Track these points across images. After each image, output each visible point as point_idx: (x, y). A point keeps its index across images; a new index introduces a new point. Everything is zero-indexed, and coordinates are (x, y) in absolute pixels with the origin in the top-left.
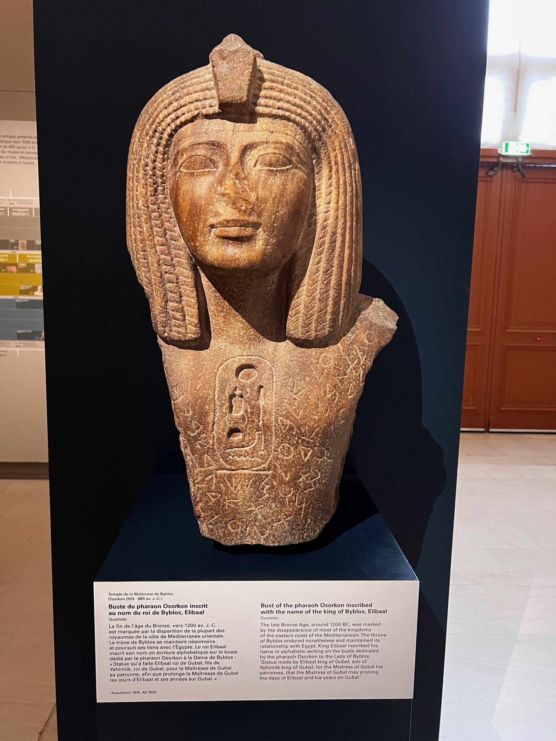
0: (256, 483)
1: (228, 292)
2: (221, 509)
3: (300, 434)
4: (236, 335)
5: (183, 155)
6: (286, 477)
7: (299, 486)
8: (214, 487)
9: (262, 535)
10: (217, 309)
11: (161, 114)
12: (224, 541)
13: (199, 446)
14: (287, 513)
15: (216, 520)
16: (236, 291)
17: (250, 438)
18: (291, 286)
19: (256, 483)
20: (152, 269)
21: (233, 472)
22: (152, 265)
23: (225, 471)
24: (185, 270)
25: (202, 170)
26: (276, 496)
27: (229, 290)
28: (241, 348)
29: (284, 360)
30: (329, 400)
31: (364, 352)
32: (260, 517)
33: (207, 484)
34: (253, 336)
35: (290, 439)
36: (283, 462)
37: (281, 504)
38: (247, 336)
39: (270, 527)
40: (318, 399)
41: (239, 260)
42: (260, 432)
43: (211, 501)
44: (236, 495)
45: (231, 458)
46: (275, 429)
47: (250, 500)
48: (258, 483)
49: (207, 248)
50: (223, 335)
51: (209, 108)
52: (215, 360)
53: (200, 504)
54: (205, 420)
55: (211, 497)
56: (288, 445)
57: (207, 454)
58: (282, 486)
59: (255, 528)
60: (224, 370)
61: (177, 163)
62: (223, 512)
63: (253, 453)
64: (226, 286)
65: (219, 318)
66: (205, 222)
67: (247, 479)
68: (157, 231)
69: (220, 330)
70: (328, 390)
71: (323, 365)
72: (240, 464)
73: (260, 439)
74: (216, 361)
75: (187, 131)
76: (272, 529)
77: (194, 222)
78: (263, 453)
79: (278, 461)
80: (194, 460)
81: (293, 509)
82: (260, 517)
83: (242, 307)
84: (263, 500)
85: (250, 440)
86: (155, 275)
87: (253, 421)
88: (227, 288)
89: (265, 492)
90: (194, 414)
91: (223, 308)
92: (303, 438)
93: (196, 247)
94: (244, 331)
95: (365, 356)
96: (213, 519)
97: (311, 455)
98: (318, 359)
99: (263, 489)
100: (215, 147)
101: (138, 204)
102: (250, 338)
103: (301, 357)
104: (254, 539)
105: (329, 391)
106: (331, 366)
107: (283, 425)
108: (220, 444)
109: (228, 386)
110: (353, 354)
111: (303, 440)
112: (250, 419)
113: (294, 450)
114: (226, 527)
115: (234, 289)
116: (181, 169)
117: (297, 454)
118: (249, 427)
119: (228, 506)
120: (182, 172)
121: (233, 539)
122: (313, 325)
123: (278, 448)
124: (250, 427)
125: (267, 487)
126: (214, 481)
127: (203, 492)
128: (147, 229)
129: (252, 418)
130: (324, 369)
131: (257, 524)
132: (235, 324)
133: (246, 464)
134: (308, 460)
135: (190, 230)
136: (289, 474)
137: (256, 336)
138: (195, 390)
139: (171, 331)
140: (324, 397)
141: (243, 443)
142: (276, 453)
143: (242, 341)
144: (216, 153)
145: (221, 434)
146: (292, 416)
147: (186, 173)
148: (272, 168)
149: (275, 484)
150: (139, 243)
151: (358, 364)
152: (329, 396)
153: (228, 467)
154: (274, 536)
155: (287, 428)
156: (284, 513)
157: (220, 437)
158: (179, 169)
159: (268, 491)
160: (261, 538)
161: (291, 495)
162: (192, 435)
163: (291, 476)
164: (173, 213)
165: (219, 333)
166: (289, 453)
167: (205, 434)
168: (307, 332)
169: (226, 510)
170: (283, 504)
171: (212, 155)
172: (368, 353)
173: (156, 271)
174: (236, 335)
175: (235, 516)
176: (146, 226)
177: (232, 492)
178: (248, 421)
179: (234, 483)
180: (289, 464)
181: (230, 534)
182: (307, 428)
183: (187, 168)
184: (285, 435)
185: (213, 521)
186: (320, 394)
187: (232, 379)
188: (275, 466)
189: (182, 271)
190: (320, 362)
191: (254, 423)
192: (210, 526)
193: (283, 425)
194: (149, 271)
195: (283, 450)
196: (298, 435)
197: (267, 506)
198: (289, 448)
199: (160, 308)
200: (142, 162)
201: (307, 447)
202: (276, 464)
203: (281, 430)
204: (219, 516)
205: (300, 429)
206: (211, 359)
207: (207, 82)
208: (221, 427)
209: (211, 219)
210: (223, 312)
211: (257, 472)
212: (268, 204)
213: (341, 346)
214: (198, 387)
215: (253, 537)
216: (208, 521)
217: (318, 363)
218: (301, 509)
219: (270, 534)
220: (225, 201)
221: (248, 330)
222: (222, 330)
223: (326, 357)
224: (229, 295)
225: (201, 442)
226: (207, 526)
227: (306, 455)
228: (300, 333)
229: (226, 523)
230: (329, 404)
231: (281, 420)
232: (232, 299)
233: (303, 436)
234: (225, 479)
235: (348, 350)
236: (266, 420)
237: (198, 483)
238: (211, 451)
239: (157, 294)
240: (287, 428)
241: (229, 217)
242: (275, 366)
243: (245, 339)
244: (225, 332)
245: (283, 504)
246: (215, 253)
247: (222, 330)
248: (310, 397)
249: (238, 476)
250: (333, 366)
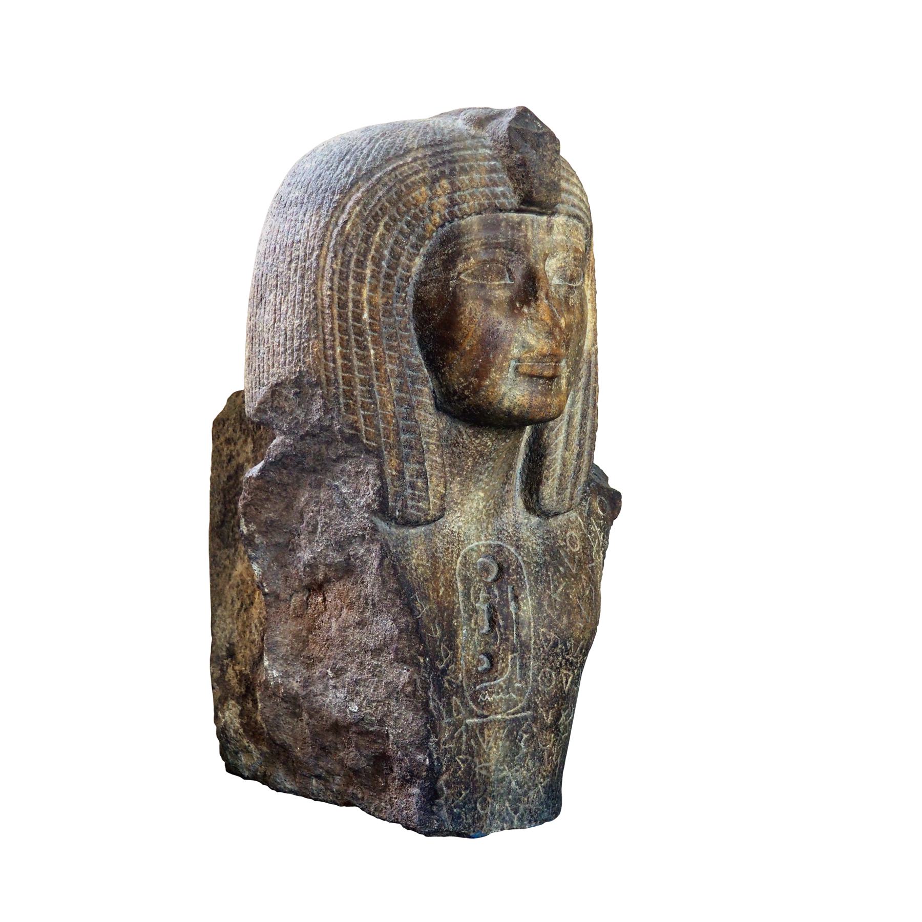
0: (512, 734)
1: (476, 447)
2: (472, 780)
3: (566, 651)
4: (473, 510)
5: (470, 259)
6: (548, 718)
7: (559, 731)
8: (463, 747)
9: (515, 813)
10: (451, 472)
11: (417, 192)
12: (474, 831)
13: (446, 685)
14: (544, 773)
15: (464, 798)
16: (489, 445)
17: (504, 665)
18: (548, 437)
19: (513, 734)
20: (382, 413)
21: (485, 720)
22: (384, 406)
23: (476, 720)
24: (428, 415)
25: (497, 283)
26: (535, 750)
27: (479, 443)
28: (478, 529)
29: (530, 544)
30: (588, 598)
31: (601, 527)
32: (513, 783)
33: (456, 744)
34: (492, 511)
35: (553, 661)
36: (545, 696)
37: (540, 761)
38: (487, 511)
39: (526, 799)
40: (579, 598)
41: (551, 406)
42: (515, 654)
43: (460, 769)
44: (489, 755)
45: (483, 699)
46: (534, 648)
47: (504, 761)
48: (515, 733)
49: (504, 389)
50: (456, 511)
51: (504, 200)
52: (450, 550)
53: (445, 777)
54: (455, 643)
55: (460, 763)
56: (550, 670)
57: (456, 697)
58: (542, 732)
59: (507, 804)
60: (464, 565)
61: (454, 268)
62: (473, 784)
63: (507, 688)
64: (477, 438)
65: (452, 486)
66: (506, 354)
67: (502, 728)
68: (390, 357)
69: (452, 504)
70: (585, 584)
71: (572, 549)
72: (493, 707)
73: (513, 665)
74: (452, 552)
75: (471, 226)
76: (528, 802)
77: (488, 354)
78: (520, 685)
79: (538, 695)
80: (441, 708)
81: (551, 766)
82: (513, 783)
83: (490, 469)
84: (520, 758)
85: (503, 669)
86: (388, 423)
87: (507, 639)
88: (477, 441)
89: (522, 744)
90: (443, 635)
91: (463, 470)
92: (567, 657)
93: (480, 386)
94: (484, 503)
95: (603, 534)
96: (461, 798)
97: (571, 683)
98: (565, 540)
99: (520, 741)
100: (513, 253)
101: (362, 314)
102: (489, 514)
103: (547, 538)
104: (506, 822)
105: (587, 587)
106: (579, 551)
107: (546, 640)
108: (469, 678)
109: (472, 589)
110: (592, 530)
111: (568, 660)
112: (504, 637)
113: (556, 677)
114: (476, 808)
115: (487, 443)
116: (462, 277)
117: (559, 683)
118: (501, 648)
119: (480, 774)
120: (464, 281)
121: (483, 827)
122: (569, 490)
123: (538, 676)
124: (504, 649)
125: (525, 736)
126: (464, 738)
127: (451, 757)
128: (375, 354)
129: (506, 634)
130: (574, 554)
131: (510, 797)
132: (475, 493)
133: (500, 705)
134: (569, 690)
135: (477, 362)
136: (550, 713)
137: (495, 510)
138: (438, 596)
139: (406, 507)
140: (583, 595)
141: (496, 674)
142: (535, 684)
143: (480, 518)
144: (513, 261)
145: (471, 663)
146: (556, 625)
147: (471, 283)
148: (572, 285)
149: (535, 730)
150: (356, 373)
151: (599, 544)
152: (587, 592)
153: (479, 712)
154: (530, 812)
155: (551, 643)
156: (542, 775)
157: (471, 667)
158: (458, 276)
159: (527, 744)
160: (514, 818)
161: (550, 746)
162: (440, 667)
163: (553, 716)
164: (413, 331)
165: (450, 509)
166: (550, 681)
167: (453, 665)
168: (562, 501)
169: (477, 780)
170: (541, 759)
171: (508, 263)
172: (604, 528)
173: (391, 416)
174: (473, 510)
175: (485, 791)
176: (374, 349)
177: (485, 752)
178: (502, 639)
179: (486, 738)
180: (552, 699)
181: (480, 818)
182: (573, 641)
183: (475, 277)
184: (549, 655)
185: (462, 801)
186: (580, 591)
187: (475, 577)
188: (535, 703)
189: (425, 416)
190: (568, 544)
191: (508, 642)
192: (455, 810)
193: (546, 640)
194: (377, 416)
195: (543, 678)
196: (562, 654)
197: (524, 766)
198: (551, 675)
199: (394, 473)
200: (373, 252)
201: (569, 670)
202: (537, 700)
203: (544, 648)
204: (468, 792)
205: (565, 645)
206: (445, 548)
207: (489, 160)
208: (471, 653)
209: (515, 350)
210: (461, 476)
211: (513, 717)
212: (573, 333)
213: (581, 521)
214: (441, 593)
215: (504, 818)
216: (453, 802)
217: (566, 546)
218: (556, 766)
219: (525, 809)
220: (537, 328)
221: (488, 502)
222: (456, 503)
223: (571, 536)
224: (477, 451)
225: (449, 677)
226: (450, 812)
227: (567, 682)
228: (555, 504)
229: (476, 803)
230: (590, 603)
231: (544, 634)
232: (480, 457)
233: (568, 654)
234: (477, 732)
235: (588, 526)
236: (525, 635)
237: (444, 743)
238: (459, 690)
239: (389, 452)
240: (551, 643)
241: (546, 350)
242: (522, 554)
243: (483, 516)
244: (459, 506)
245: (541, 759)
246: (518, 397)
247: (456, 503)
248: (571, 597)
249: (492, 726)
250: (581, 551)
